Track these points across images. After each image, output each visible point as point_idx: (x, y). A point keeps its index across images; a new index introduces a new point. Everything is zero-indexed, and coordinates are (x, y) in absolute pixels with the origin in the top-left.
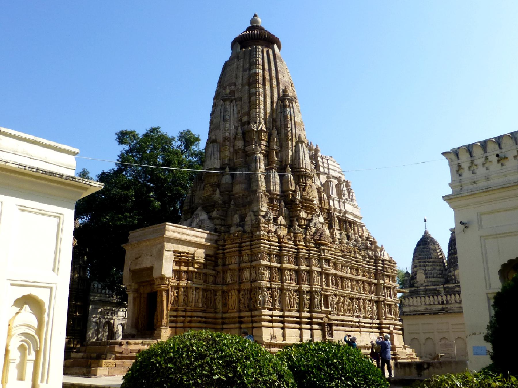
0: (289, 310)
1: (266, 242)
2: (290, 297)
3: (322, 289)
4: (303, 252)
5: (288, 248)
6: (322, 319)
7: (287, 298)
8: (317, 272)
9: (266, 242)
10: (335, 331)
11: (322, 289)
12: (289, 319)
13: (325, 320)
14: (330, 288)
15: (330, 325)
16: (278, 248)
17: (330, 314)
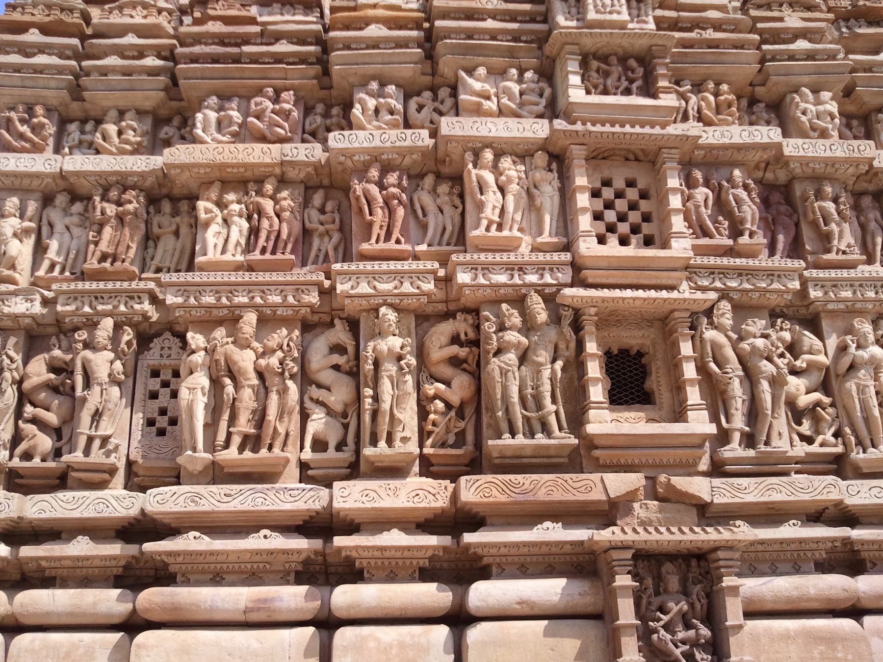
0: (217, 474)
1: (33, 36)
2: (222, 373)
3: (576, 267)
4: (375, 44)
5: (246, 40)
6: (607, 513)
7: (201, 380)
8: (523, 153)
9: (33, 36)
10: (749, 615)
11: (576, 267)
12: (192, 542)
13: (646, 527)
14: (681, 247)
15: (698, 568)
16: (151, 61)
17: (718, 470)
